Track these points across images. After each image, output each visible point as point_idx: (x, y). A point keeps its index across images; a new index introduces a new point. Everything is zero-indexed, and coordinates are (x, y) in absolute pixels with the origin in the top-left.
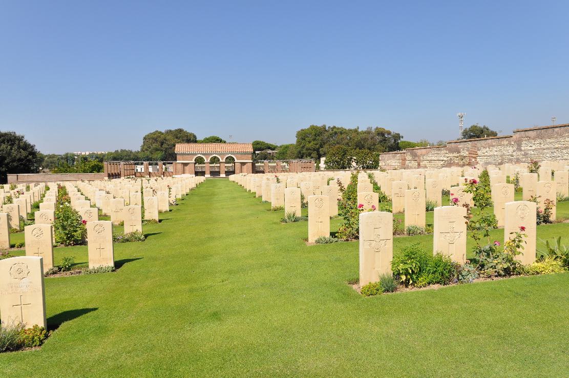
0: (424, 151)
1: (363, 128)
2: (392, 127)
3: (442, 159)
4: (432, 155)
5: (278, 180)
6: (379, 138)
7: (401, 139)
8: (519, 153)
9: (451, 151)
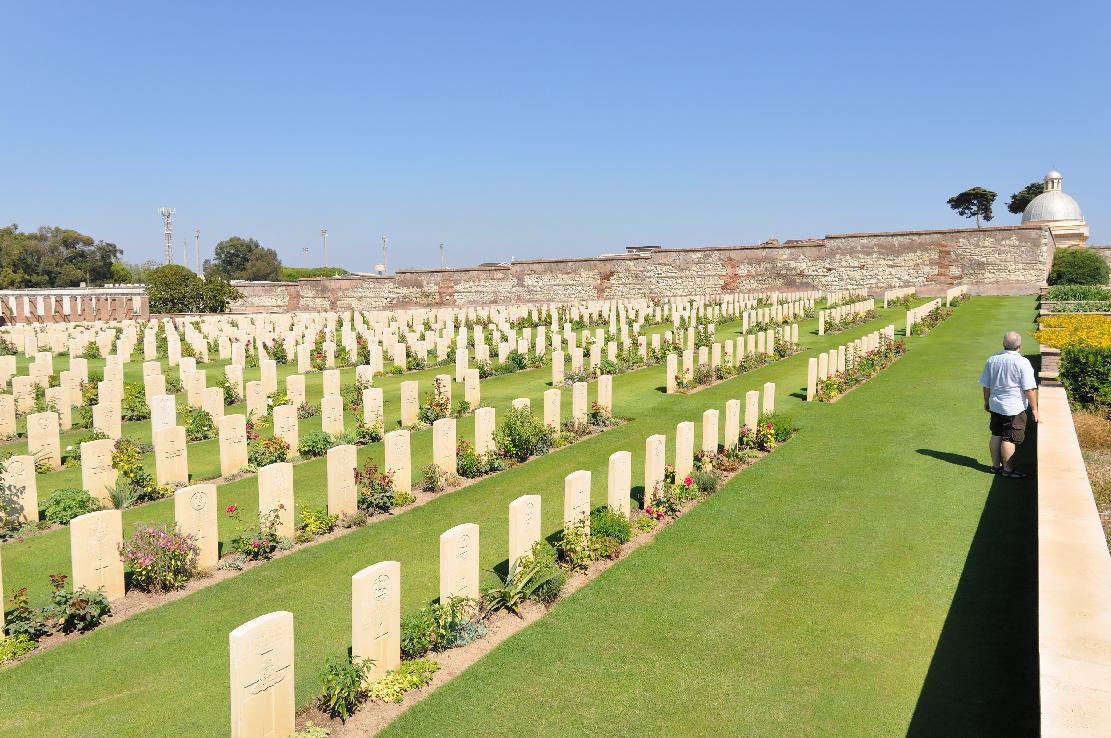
0: (345, 284)
1: (28, 228)
2: (97, 230)
3: (386, 296)
4: (368, 291)
5: (253, 323)
6: (65, 252)
7: (118, 255)
8: (521, 289)
9: (403, 284)
